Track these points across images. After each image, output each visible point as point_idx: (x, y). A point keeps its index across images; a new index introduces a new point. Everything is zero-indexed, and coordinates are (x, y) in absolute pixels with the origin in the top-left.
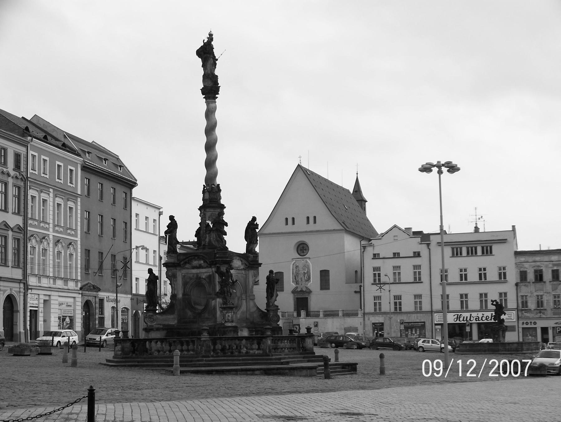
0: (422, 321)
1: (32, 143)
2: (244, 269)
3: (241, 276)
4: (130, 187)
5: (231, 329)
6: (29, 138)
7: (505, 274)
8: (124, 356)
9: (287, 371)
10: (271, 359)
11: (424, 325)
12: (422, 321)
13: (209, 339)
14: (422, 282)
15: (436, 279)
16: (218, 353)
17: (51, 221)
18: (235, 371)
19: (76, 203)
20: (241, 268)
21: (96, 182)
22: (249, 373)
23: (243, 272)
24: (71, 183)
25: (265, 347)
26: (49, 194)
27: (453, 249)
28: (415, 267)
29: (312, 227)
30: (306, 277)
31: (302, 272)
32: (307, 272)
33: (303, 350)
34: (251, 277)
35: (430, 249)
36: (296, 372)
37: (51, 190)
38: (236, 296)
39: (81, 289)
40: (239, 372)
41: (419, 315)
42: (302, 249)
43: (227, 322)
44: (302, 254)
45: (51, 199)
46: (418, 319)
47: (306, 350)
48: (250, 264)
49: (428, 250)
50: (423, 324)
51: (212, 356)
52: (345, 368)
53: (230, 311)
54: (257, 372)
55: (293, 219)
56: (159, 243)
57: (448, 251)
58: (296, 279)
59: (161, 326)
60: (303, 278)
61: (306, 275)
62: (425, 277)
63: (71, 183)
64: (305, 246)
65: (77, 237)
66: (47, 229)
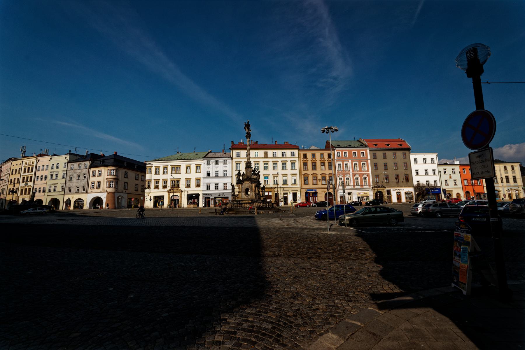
56: (438, 166)
65: (369, 172)
66: (349, 172)
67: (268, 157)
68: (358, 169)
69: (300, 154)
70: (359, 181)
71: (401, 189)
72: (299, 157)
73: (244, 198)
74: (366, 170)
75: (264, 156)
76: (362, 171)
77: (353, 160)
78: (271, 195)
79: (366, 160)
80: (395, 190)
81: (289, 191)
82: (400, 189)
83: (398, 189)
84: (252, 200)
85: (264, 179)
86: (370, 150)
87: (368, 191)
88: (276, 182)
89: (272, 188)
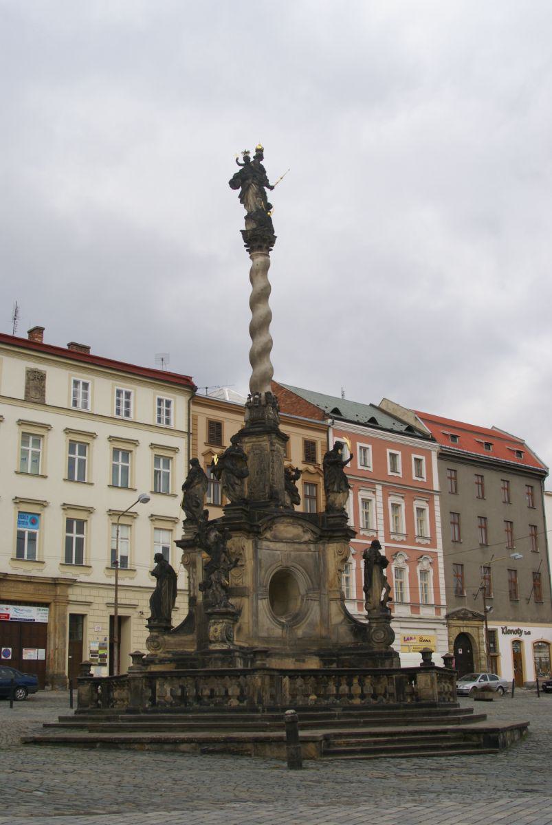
1: (334, 426)
2: (315, 542)
3: (308, 555)
4: (540, 478)
5: (217, 655)
6: (330, 421)
8: (80, 709)
9: (249, 746)
10: (253, 719)
13: (141, 676)
16: (191, 704)
17: (381, 528)
18: (172, 743)
19: (430, 502)
20: (303, 540)
21: (467, 474)
22: (167, 747)
23: (312, 547)
24: (419, 475)
25: (251, 693)
26: (374, 492)
33: (412, 699)
34: (333, 555)
36: (267, 748)
37: (379, 488)
38: (300, 594)
39: (447, 617)
40: (147, 747)
43: (214, 642)
45: (380, 499)
47: (417, 700)
48: (323, 531)
51: (145, 711)
52: (470, 740)
53: (221, 621)
54: (183, 747)
59: (170, 656)
63: (419, 475)
65: (435, 547)
67: (43, 404)
68: (404, 532)
69: (195, 419)
70: (407, 585)
71: (524, 627)
72: (188, 433)
73: (264, 634)
74: (426, 538)
75: (27, 393)
76: (417, 540)
77: (391, 487)
78: (45, 625)
79: (427, 494)
80: (511, 632)
81: (139, 609)
82: (521, 628)
83: (517, 628)
84: (325, 655)
85: (19, 523)
86: (442, 456)
87: (432, 632)
88: (75, 553)
89: (55, 583)
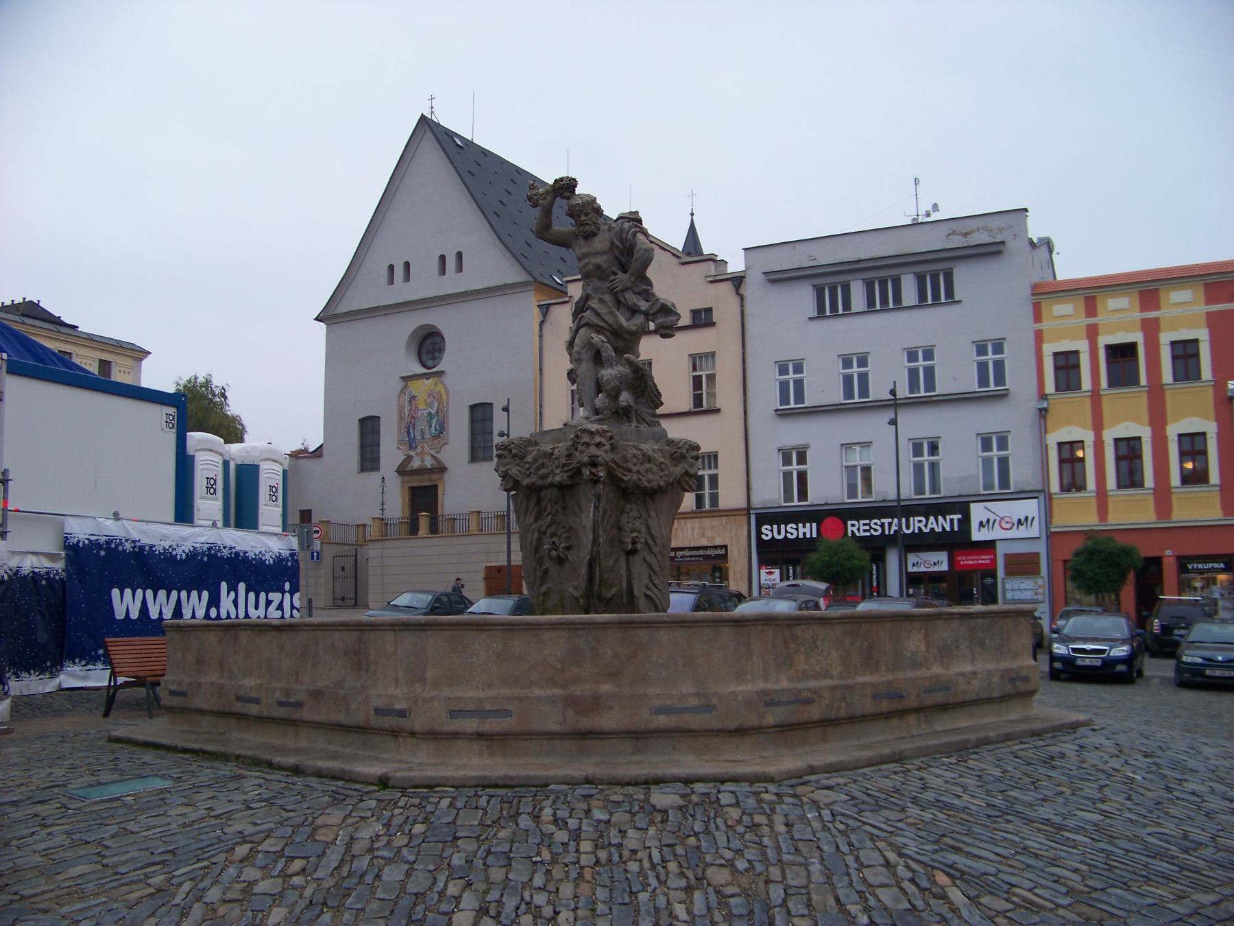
0: (718, 542)
7: (999, 366)
11: (724, 557)
12: (718, 543)
14: (718, 411)
15: (766, 397)
27: (819, 292)
28: (696, 360)
29: (452, 283)
30: (433, 426)
31: (423, 412)
32: (437, 412)
35: (742, 298)
41: (707, 522)
42: (430, 348)
44: (430, 363)
46: (703, 536)
49: (735, 301)
50: (723, 552)
55: (407, 265)
57: (803, 298)
58: (408, 432)
60: (427, 429)
61: (434, 421)
62: (726, 394)
64: (438, 340)
